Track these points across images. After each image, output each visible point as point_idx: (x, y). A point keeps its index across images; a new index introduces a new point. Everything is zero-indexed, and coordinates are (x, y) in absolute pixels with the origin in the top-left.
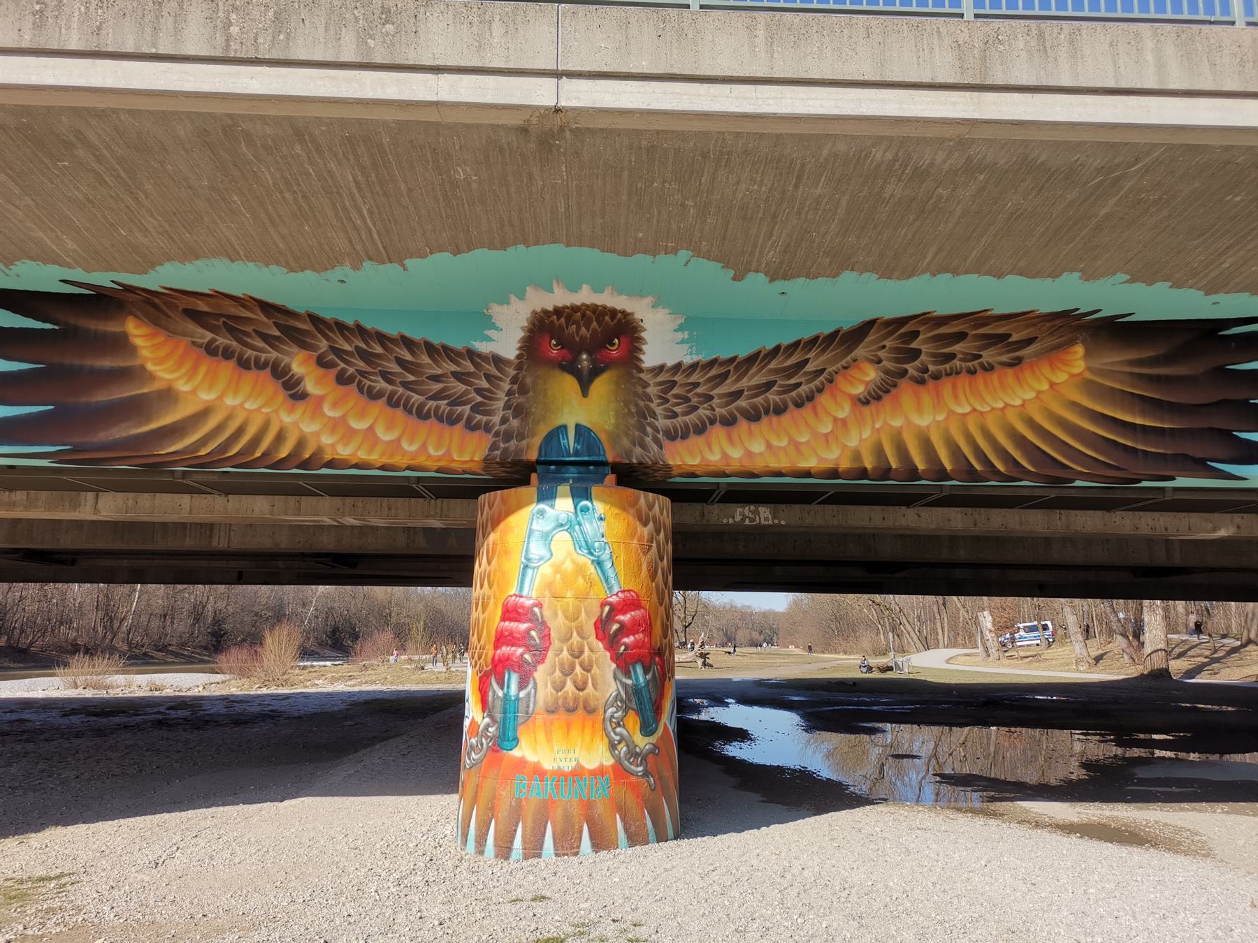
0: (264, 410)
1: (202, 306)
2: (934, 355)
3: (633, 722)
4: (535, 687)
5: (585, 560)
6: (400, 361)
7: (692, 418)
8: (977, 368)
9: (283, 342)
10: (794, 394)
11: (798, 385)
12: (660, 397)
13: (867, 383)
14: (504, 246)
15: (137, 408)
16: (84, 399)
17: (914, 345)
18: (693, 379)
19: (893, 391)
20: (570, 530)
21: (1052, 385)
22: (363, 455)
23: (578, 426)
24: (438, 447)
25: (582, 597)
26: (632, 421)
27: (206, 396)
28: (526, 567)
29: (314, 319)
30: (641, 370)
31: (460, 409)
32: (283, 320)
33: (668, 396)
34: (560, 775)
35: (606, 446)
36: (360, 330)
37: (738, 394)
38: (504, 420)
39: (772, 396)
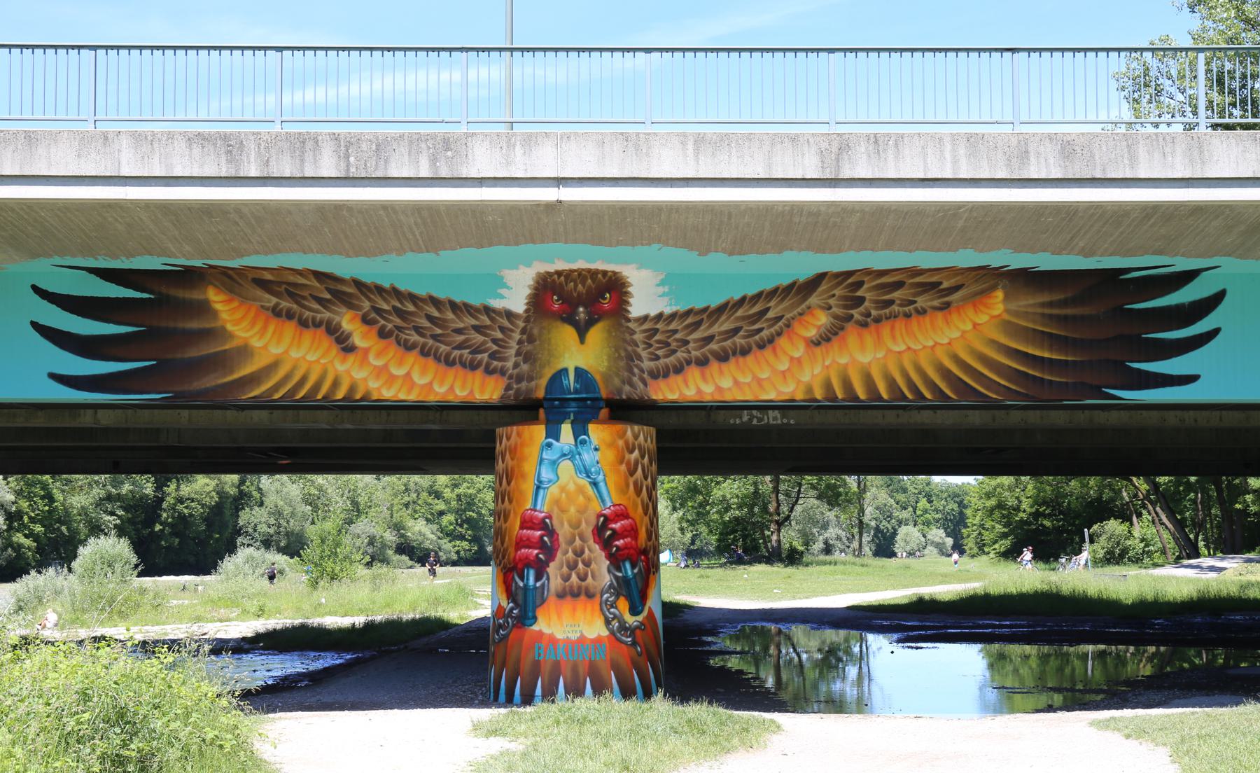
0: (322, 361)
1: (268, 277)
2: (877, 302)
3: (623, 605)
4: (548, 579)
5: (584, 482)
6: (430, 318)
7: (672, 359)
8: (913, 313)
9: (334, 304)
10: (757, 337)
11: (760, 330)
12: (645, 343)
13: (819, 327)
14: (517, 244)
15: (222, 361)
16: (179, 356)
17: (859, 294)
18: (672, 326)
19: (841, 333)
20: (572, 459)
21: (975, 325)
22: (402, 396)
23: (577, 369)
24: (463, 387)
25: (582, 511)
26: (622, 364)
27: (275, 350)
28: (538, 488)
29: (358, 283)
30: (629, 320)
31: (479, 356)
32: (332, 286)
33: (652, 342)
34: (568, 641)
35: (601, 385)
36: (395, 292)
37: (709, 339)
38: (516, 365)
39: (739, 340)
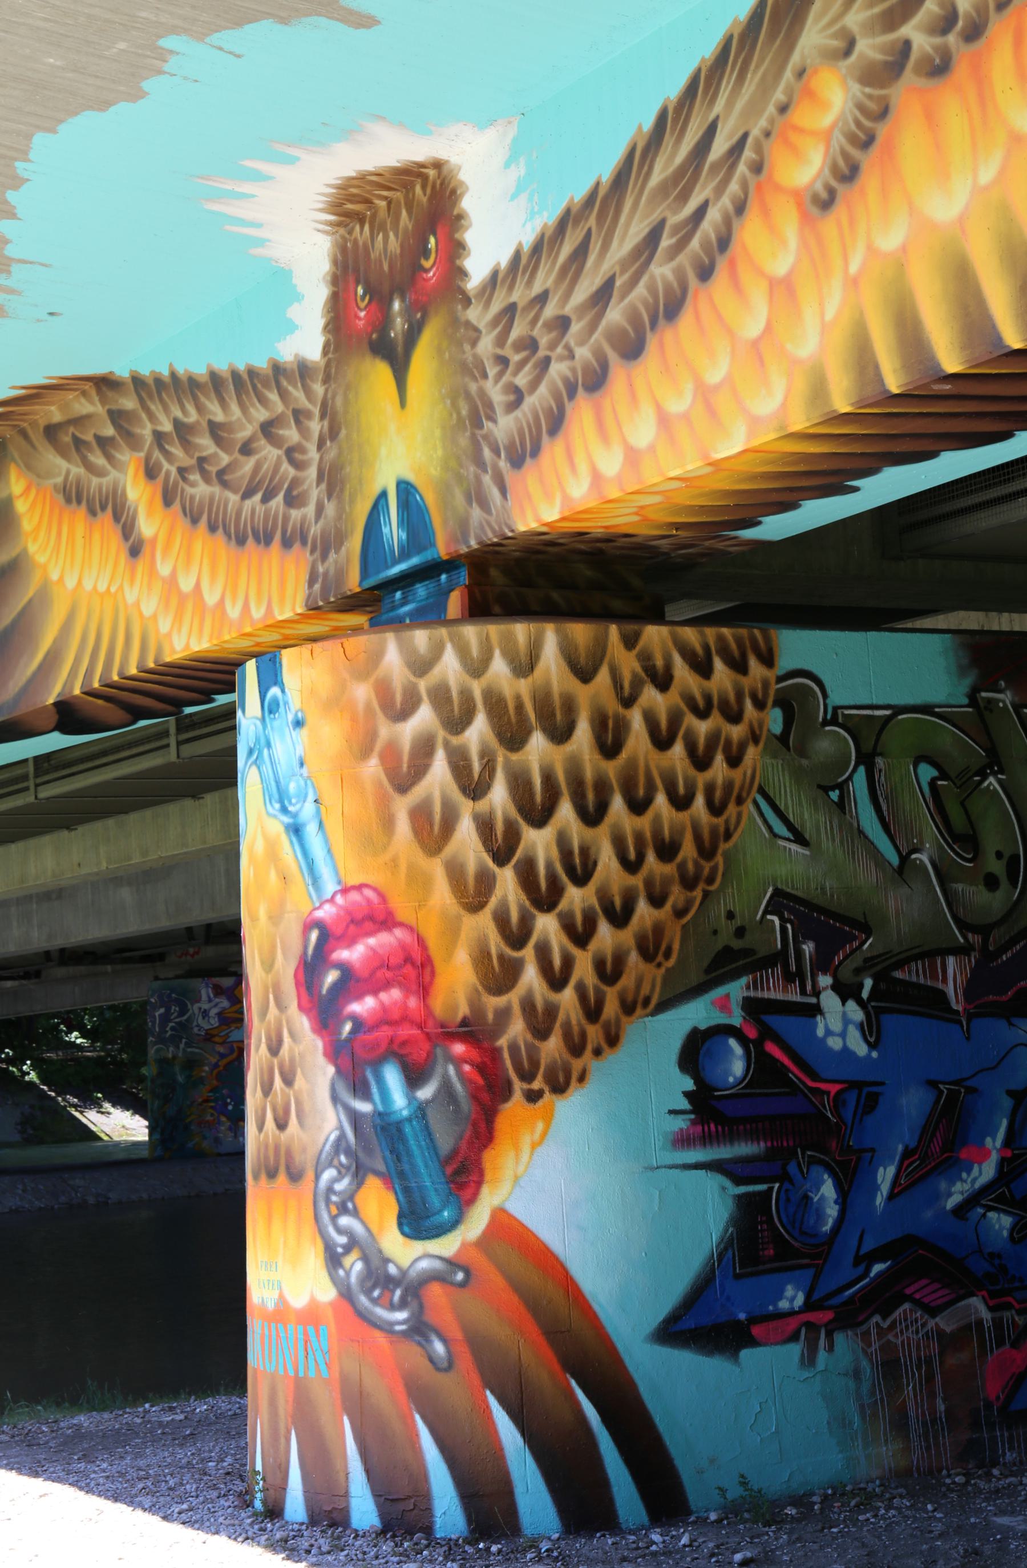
3: (379, 1205)
